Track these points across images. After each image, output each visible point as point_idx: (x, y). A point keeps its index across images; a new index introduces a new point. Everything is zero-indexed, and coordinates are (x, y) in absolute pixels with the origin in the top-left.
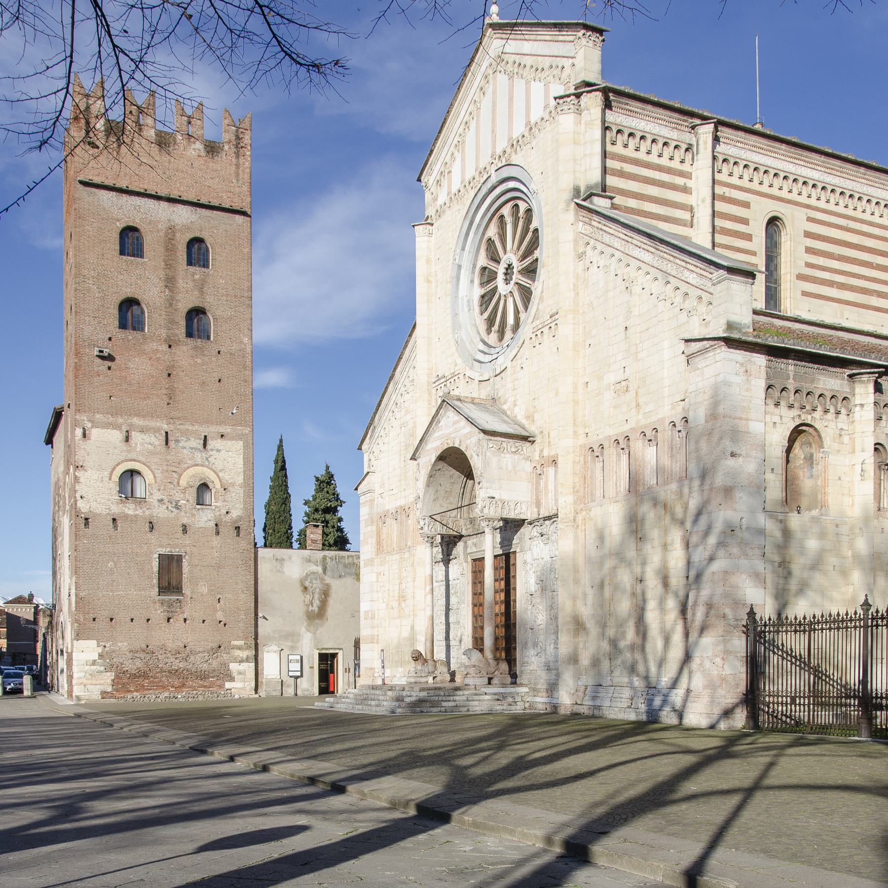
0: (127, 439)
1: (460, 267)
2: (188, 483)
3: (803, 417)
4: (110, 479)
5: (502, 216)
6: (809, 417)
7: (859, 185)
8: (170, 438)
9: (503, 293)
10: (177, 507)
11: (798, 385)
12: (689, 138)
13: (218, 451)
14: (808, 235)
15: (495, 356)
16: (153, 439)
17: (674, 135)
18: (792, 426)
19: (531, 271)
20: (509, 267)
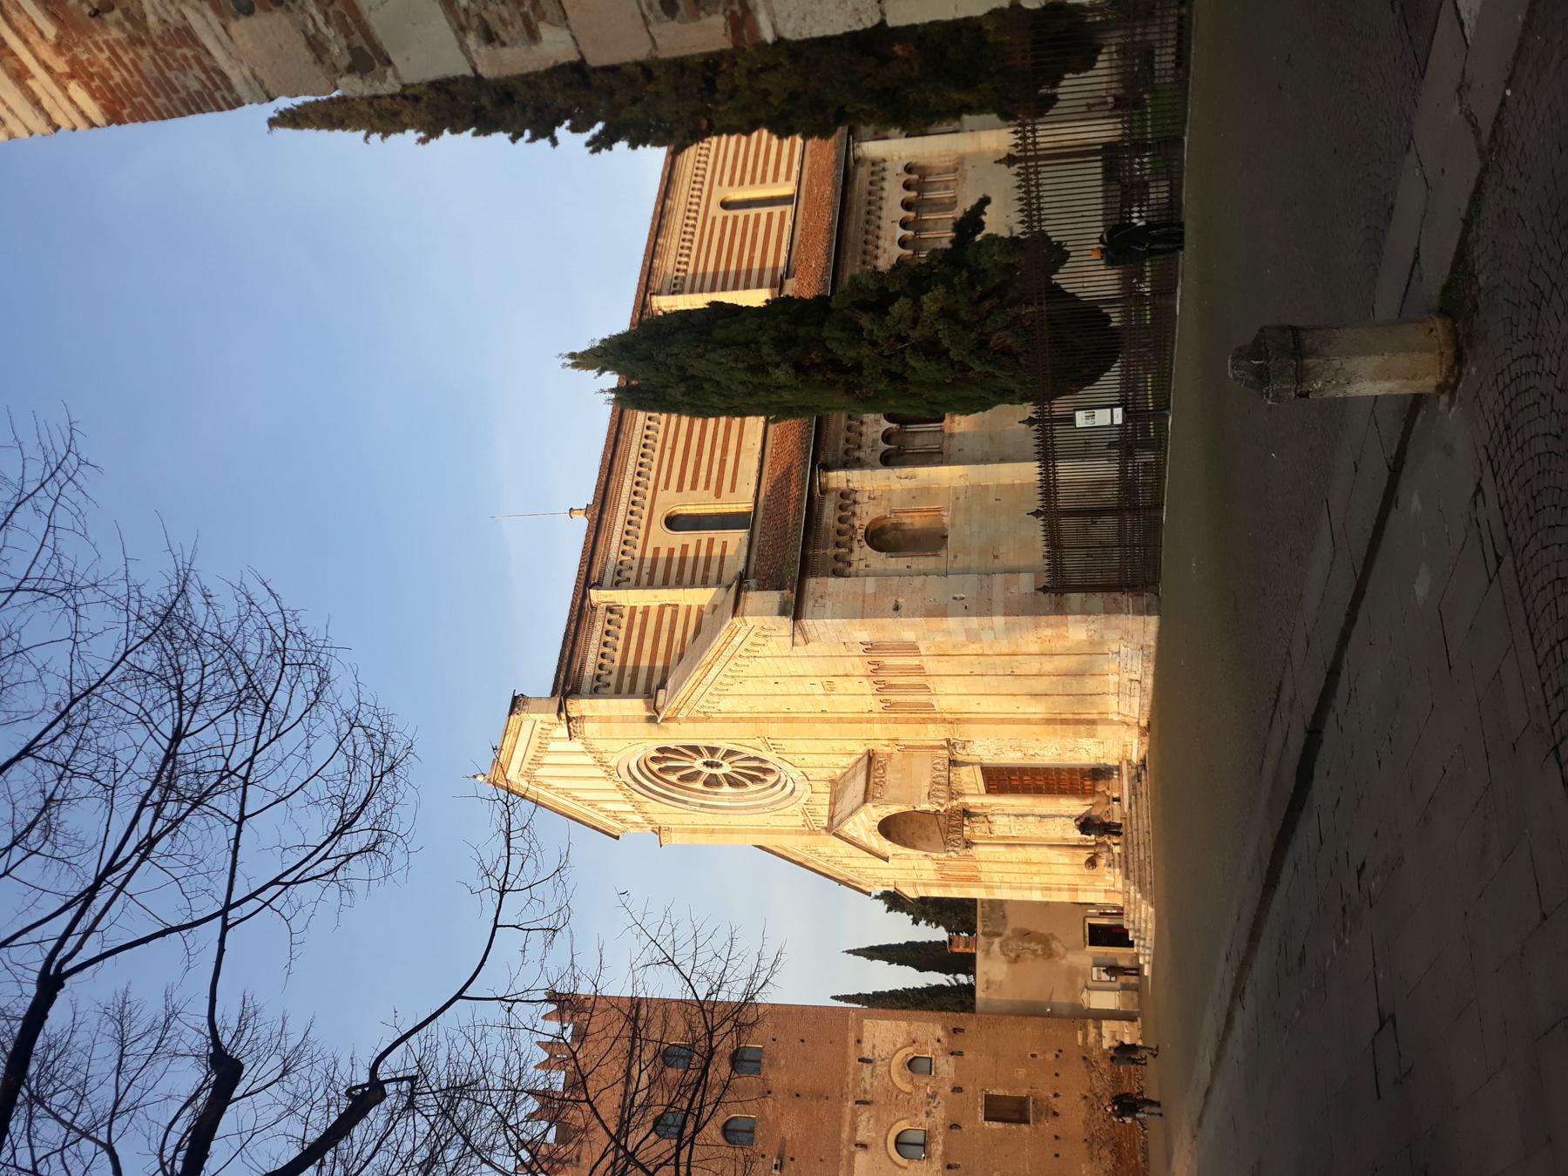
0: (864, 1146)
1: (702, 805)
2: (909, 1083)
3: (860, 538)
4: (905, 1168)
5: (660, 770)
6: (859, 531)
7: (634, 439)
8: (862, 1098)
9: (730, 769)
10: (934, 1096)
11: (831, 545)
12: (600, 612)
13: (874, 1047)
14: (680, 488)
15: (789, 779)
16: (864, 1118)
17: (599, 625)
18: (868, 549)
19: (713, 751)
20: (706, 764)
